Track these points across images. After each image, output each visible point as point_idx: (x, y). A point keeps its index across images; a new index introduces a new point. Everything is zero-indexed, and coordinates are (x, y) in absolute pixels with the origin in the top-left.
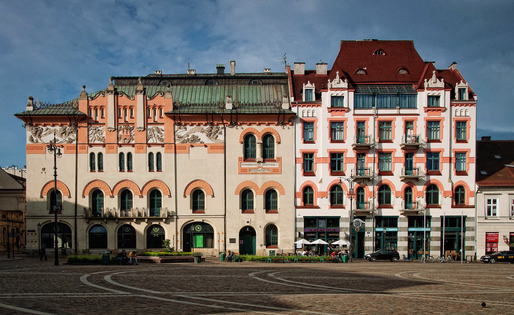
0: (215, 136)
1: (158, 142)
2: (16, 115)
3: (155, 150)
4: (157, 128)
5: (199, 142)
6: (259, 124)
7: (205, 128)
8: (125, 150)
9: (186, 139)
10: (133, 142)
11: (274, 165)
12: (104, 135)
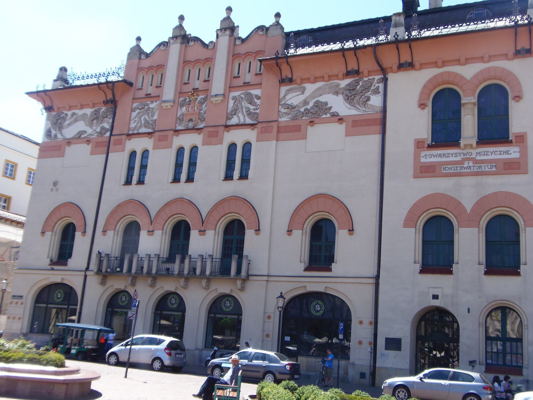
0: (363, 99)
1: (249, 121)
2: (29, 94)
3: (239, 137)
4: (250, 93)
5: (328, 115)
6: (467, 61)
7: (344, 83)
8: (187, 141)
9: (302, 110)
10: (201, 126)
11: (507, 153)
12: (155, 117)
